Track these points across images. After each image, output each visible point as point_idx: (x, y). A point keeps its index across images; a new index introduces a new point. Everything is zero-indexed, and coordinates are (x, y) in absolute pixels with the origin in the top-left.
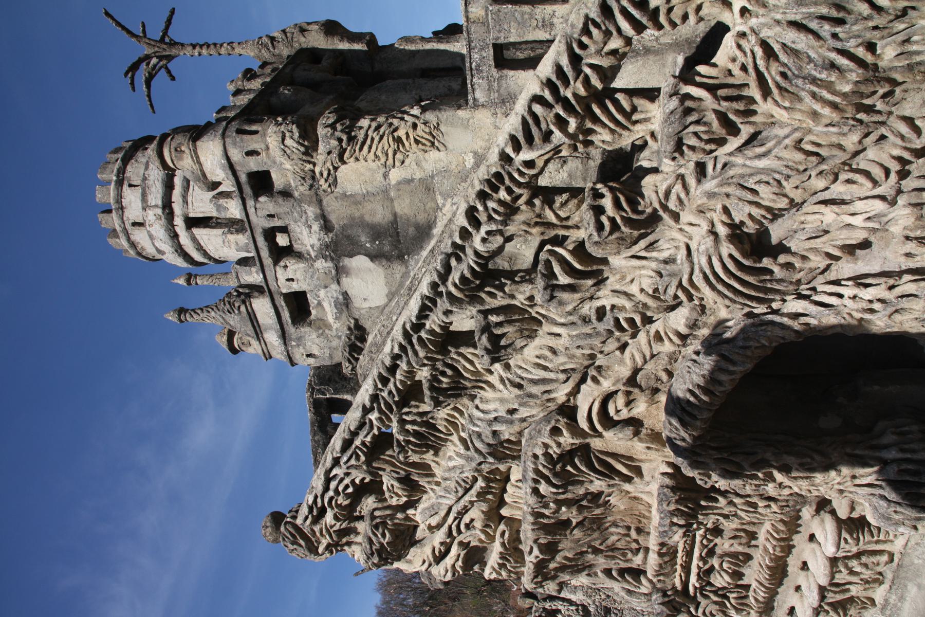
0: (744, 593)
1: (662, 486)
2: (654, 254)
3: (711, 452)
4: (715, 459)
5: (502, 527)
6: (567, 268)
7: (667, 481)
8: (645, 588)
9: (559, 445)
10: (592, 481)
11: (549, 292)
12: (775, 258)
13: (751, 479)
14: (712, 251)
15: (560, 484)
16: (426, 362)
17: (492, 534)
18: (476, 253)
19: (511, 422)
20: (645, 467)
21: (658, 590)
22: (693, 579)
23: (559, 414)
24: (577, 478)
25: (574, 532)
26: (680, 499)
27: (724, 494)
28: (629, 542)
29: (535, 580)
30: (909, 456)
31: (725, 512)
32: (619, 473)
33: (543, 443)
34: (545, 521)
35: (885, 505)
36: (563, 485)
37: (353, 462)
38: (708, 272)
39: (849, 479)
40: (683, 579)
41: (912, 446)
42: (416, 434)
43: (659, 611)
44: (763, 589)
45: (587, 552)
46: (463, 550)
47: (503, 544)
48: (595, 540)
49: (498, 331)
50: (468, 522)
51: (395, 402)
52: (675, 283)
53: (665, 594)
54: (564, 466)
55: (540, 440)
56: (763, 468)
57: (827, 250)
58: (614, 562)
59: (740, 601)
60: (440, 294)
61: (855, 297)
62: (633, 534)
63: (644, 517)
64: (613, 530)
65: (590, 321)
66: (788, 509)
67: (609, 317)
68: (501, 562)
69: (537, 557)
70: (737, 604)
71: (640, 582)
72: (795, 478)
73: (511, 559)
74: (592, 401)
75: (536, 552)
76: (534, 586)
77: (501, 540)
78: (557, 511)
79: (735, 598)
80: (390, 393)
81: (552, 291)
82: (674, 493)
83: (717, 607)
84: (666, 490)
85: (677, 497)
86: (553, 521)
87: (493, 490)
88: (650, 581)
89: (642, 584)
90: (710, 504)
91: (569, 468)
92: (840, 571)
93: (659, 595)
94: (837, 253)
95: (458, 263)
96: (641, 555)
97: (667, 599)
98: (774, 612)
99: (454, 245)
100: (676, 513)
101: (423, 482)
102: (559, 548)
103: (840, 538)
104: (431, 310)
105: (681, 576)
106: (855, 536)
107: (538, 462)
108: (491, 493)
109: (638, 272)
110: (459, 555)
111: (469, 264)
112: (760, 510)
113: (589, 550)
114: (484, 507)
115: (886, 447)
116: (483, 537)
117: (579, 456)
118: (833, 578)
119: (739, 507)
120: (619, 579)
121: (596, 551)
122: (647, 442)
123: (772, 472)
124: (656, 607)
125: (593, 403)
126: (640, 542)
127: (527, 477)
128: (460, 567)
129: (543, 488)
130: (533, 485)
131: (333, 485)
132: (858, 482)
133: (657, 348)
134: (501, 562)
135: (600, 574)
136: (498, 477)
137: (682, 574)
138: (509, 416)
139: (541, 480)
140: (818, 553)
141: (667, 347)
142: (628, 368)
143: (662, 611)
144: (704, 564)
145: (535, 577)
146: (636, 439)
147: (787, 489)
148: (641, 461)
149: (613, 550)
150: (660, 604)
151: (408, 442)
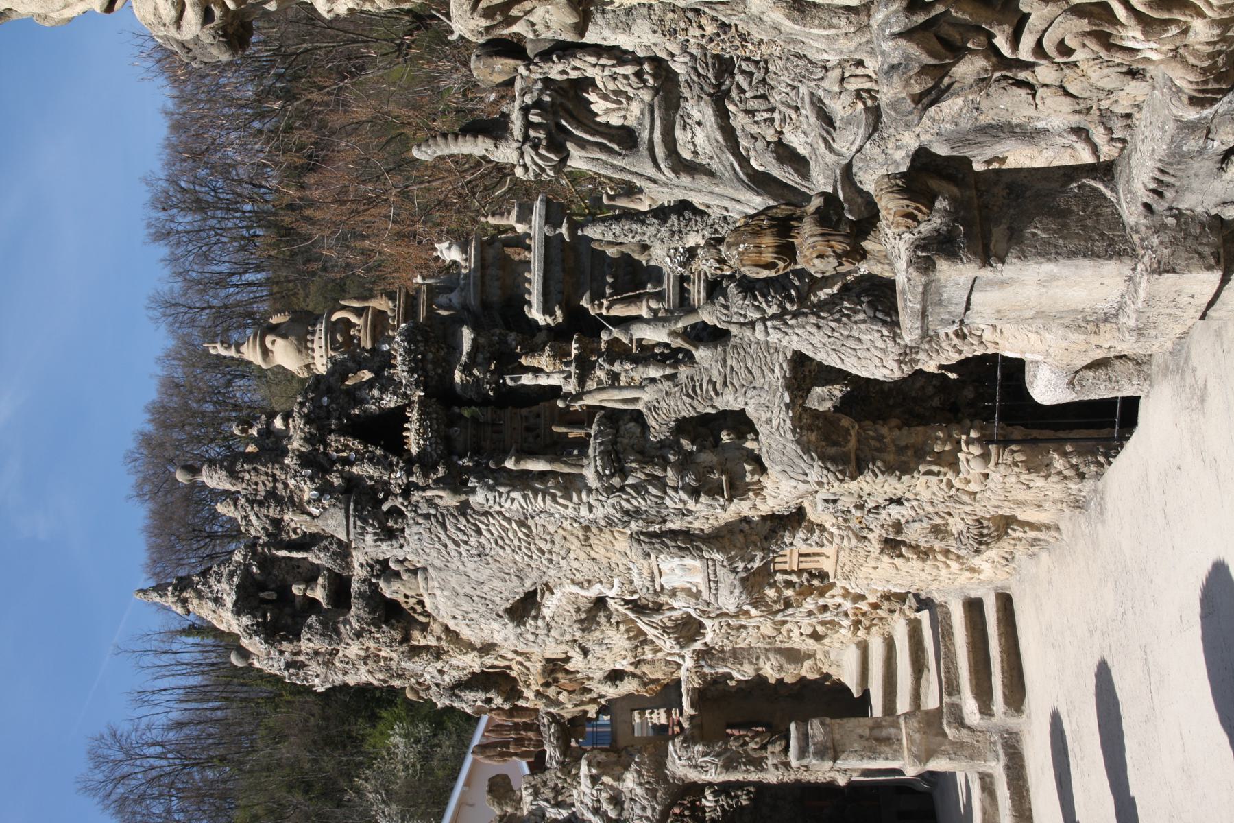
43: (895, 59)
76: (485, 23)
83: (1084, 24)
97: (920, 18)
124: (887, 46)
143: (907, 58)
150: (900, 35)
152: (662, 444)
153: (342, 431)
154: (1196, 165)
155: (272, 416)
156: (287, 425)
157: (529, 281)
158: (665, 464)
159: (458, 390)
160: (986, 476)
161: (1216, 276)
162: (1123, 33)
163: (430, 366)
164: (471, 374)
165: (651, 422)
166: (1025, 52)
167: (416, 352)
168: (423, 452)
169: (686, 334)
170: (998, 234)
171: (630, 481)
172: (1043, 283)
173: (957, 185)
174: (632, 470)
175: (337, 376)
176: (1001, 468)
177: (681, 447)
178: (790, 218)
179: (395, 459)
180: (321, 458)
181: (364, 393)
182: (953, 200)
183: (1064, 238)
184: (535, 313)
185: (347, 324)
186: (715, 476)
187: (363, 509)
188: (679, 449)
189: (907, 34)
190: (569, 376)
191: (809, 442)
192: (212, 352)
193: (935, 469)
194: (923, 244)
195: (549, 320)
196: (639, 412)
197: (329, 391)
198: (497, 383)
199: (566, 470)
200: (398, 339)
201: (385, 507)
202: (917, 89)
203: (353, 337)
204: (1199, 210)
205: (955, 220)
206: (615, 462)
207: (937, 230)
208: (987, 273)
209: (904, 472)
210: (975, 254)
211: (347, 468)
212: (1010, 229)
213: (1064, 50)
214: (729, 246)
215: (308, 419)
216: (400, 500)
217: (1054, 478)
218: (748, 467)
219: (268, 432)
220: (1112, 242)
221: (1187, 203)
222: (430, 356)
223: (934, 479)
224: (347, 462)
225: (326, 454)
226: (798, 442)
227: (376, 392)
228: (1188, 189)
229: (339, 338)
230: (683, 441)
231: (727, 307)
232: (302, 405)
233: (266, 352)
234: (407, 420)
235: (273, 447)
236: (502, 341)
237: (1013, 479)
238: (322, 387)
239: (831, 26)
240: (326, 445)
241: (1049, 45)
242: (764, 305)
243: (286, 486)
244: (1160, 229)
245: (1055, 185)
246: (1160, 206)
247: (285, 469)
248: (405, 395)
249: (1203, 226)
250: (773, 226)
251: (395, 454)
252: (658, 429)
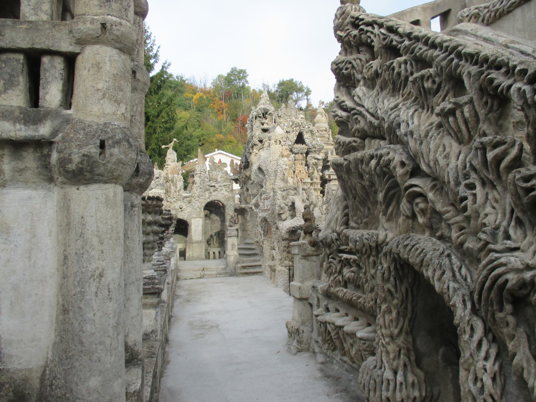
2: (513, 223)
5: (358, 140)
11: (480, 146)
12: (512, 314)
14: (510, 266)
16: (439, 68)
18: (510, 87)
22: (345, 256)
30: (398, 387)
37: (382, 37)
38: (495, 263)
41: (404, 390)
42: (399, 74)
47: (350, 143)
49: (458, 113)
51: (416, 54)
52: (489, 239)
57: (518, 355)
60: (482, 66)
65: (466, 179)
67: (468, 193)
68: (341, 143)
74: (421, 186)
80: (420, 49)
95: (503, 74)
99: (515, 67)
101: (377, 87)
104: (471, 63)
105: (347, 249)
109: (500, 211)
111: (503, 82)
114: (366, 128)
115: (405, 376)
125: (420, 187)
129: (373, 162)
131: (369, 28)
133: (454, 229)
141: (454, 235)
142: (440, 209)
151: (393, 69)
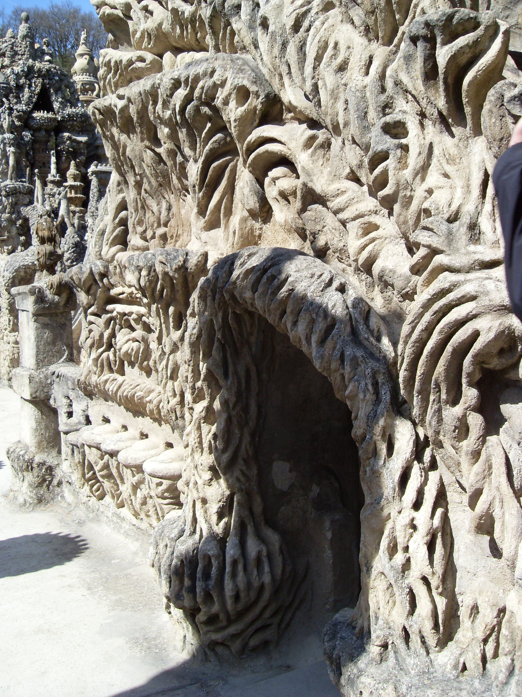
0: (115, 369)
1: (187, 254)
3: (220, 314)
4: (212, 321)
5: (149, 57)
6: (464, 60)
7: (193, 261)
8: (108, 251)
9: (226, 102)
10: (196, 161)
11: (423, 32)
13: (193, 371)
15: (187, 116)
17: (143, 47)
19: (251, 28)
20: (218, 233)
21: (107, 267)
23: (267, 96)
24: (198, 139)
25: (148, 151)
26: (171, 279)
27: (182, 339)
28: (152, 226)
29: (97, 112)
31: (165, 339)
32: (209, 197)
33: (226, 80)
34: (150, 108)
35: (173, 536)
36: (187, 120)
39: (201, 495)
40: (121, 296)
44: (115, 390)
45: (135, 175)
46: (122, 11)
47: (131, 62)
48: (150, 183)
50: (150, 8)
52: (436, 242)
53: (103, 275)
54: (210, 119)
55: (229, 74)
56: (209, 387)
58: (133, 211)
59: (105, 363)
61: (414, 527)
62: (161, 230)
63: (176, 241)
64: (164, 205)
65: (385, 115)
66: (174, 418)
67: (389, 142)
68: (112, 64)
69: (116, 106)
70: (102, 360)
71: (113, 243)
72: (199, 428)
73: (117, 77)
74: (283, 141)
75: (121, 104)
77: (134, 59)
78: (163, 122)
79: (108, 358)
81: (425, 38)
82: (176, 270)
83: (97, 338)
84: (181, 259)
85: (171, 274)
86: (152, 118)
87: (185, 32)
88: (113, 258)
89: (110, 247)
90: (171, 320)
91: (209, 125)
92: (134, 476)
93: (102, 269)
94: (481, 505)
96: (140, 243)
97: (97, 278)
98: (104, 402)
100: (152, 274)
102: (131, 136)
103: (161, 478)
105: (123, 293)
106: (166, 494)
107: (207, 78)
108: (182, 32)
110: (116, 8)
112: (170, 383)
113: (138, 177)
116: (138, 35)
117: (225, 139)
118: (127, 467)
119: (171, 357)
120: (117, 220)
121: (139, 185)
122: (241, 229)
123: (204, 399)
126: (153, 240)
127: (190, 67)
128: (104, 13)
129: (181, 93)
130: (183, 80)
132: (199, 505)
133: (354, 227)
134: (112, 64)
135: (121, 196)
136: (199, 35)
137: (125, 295)
138: (259, 21)
139: (188, 89)
140: (152, 452)
142: (325, 187)
143: (83, 273)
144: (134, 320)
145: (99, 110)
146: (246, 214)
147: (190, 417)
148: (227, 226)
149: (143, 207)
152: (19, 212)
153: (43, 85)
154: (65, 387)
155: (51, 55)
156: (46, 61)
157: (106, 166)
158: (11, 213)
159: (60, 135)
160: (9, 343)
161: (28, 397)
162: (94, 351)
163: (71, 123)
164: (67, 140)
165: (29, 208)
166: (91, 318)
167: (77, 117)
168: (34, 119)
169: (63, 222)
170: (46, 320)
171: (4, 199)
172: (29, 338)
173: (64, 304)
174: (8, 200)
175: (67, 83)
176: (12, 349)
177: (18, 220)
178: (55, 242)
179: (31, 107)
180: (32, 75)
181: (60, 95)
182: (58, 303)
183: (44, 344)
184: (92, 168)
185: (93, 90)
186: (6, 234)
187: (4, 90)
188: (17, 219)
189: (91, 273)
190: (54, 177)
191: (20, 272)
192: (83, 33)
193: (11, 323)
194: (41, 291)
195: (90, 174)
196: (33, 203)
197: (61, 80)
198: (64, 151)
199: (9, 173)
200: (83, 110)
201: (4, 100)
202: (74, 278)
203: (87, 92)
204: (53, 391)
205: (50, 303)
206: (12, 193)
207: (46, 297)
208: (31, 315)
209: (10, 310)
210: (37, 311)
211: (27, 86)
212: (48, 324)
213: (90, 331)
214: (46, 219)
215: (48, 71)
216: (7, 106)
217: (8, 369)
218: (10, 247)
219: (43, 53)
220: (42, 361)
221: (55, 386)
222: (75, 123)
223: (7, 323)
224: (30, 86)
225: (34, 77)
226: (19, 267)
227: (60, 100)
228: (60, 386)
229: (87, 87)
230: (21, 221)
231: (73, 237)
232: (55, 68)
233: (82, 55)
234: (48, 112)
235: (37, 55)
236: (81, 154)
237: (7, 354)
238: (63, 77)
239: (95, 245)
240: (37, 77)
241: (92, 326)
242: (70, 252)
243: (20, 60)
244: (46, 378)
245: (65, 341)
246: (54, 377)
247: (27, 59)
248: (59, 112)
249: (47, 392)
250: (52, 235)
251: (34, 107)
252: (25, 211)
